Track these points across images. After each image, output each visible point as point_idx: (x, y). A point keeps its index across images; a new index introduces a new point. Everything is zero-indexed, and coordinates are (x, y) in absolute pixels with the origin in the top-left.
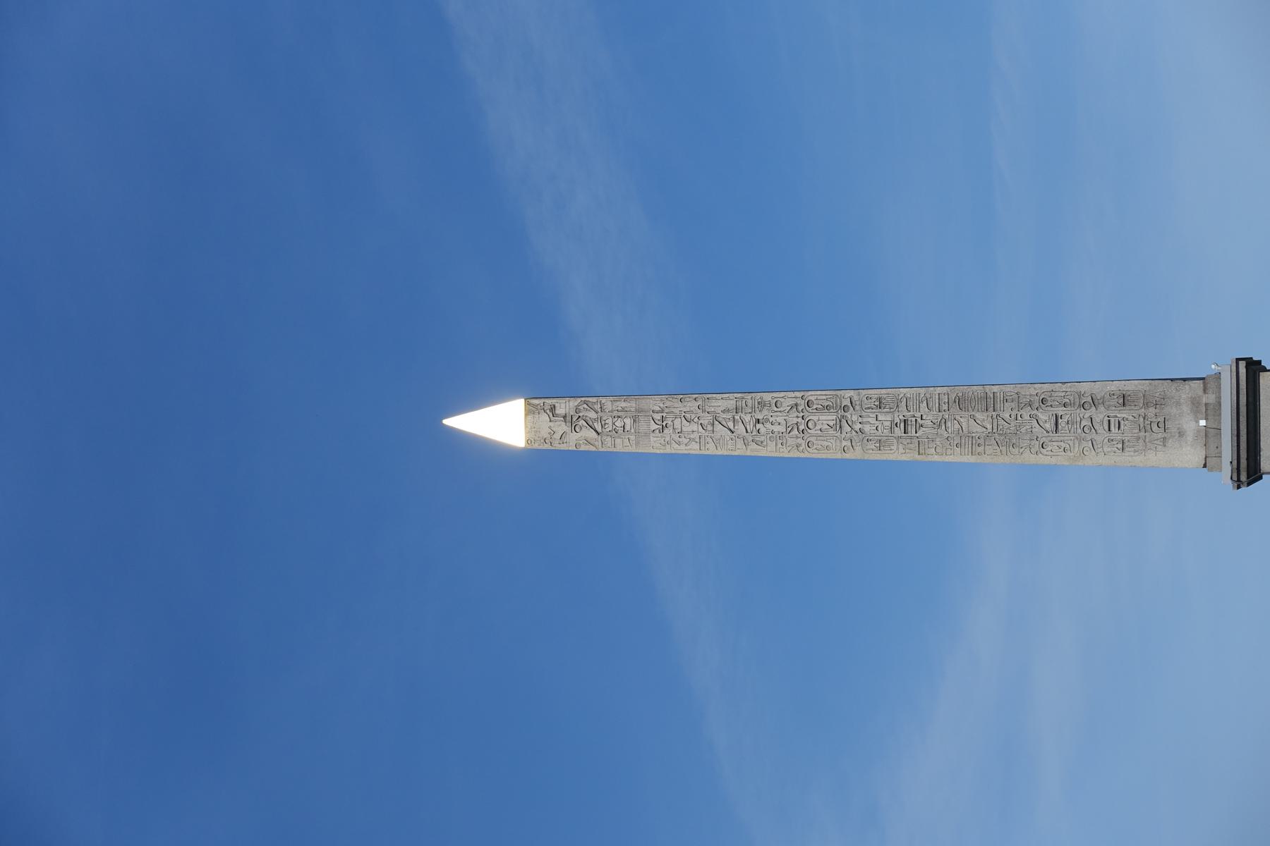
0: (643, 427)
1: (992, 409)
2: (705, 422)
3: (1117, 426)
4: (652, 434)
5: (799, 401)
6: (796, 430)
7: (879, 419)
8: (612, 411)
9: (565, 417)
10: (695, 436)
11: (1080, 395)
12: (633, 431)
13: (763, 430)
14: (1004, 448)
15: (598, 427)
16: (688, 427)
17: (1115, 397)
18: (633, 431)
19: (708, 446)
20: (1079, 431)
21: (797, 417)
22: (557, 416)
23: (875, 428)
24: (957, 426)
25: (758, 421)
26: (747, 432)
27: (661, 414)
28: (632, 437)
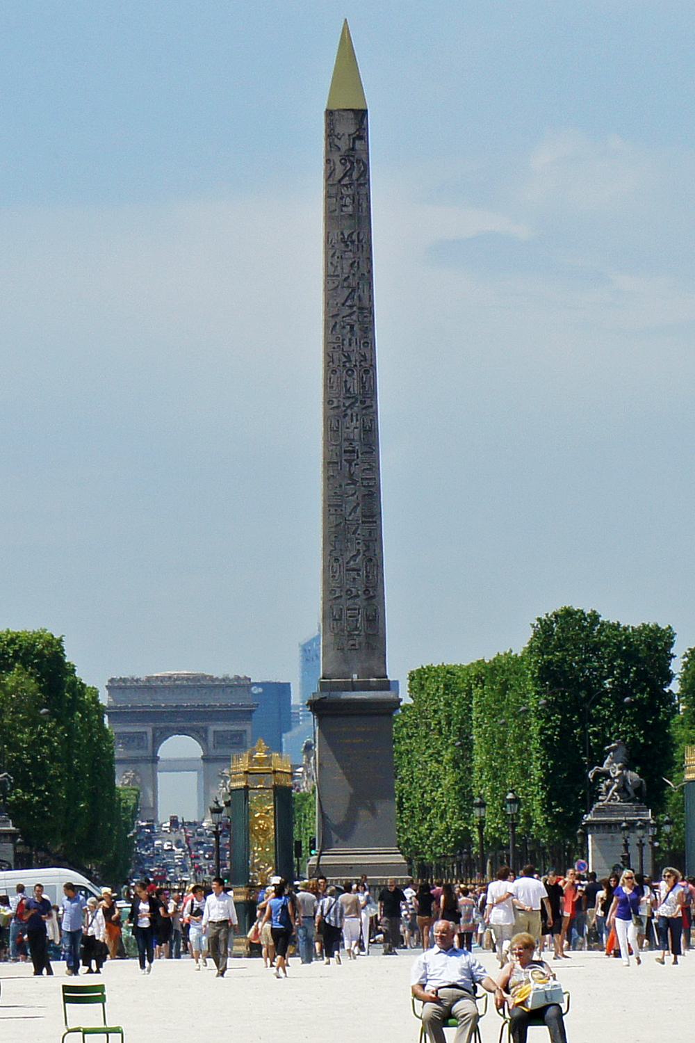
0: (346, 223)
1: (364, 519)
2: (350, 280)
3: (352, 615)
4: (339, 233)
5: (369, 362)
6: (345, 360)
7: (356, 430)
8: (358, 193)
9: (353, 149)
10: (339, 271)
11: (375, 587)
12: (343, 214)
13: (345, 331)
14: (333, 529)
15: (346, 181)
16: (346, 264)
17: (374, 613)
18: (343, 214)
19: (330, 282)
20: (348, 587)
21: (356, 361)
22: (354, 143)
23: (348, 425)
24: (350, 493)
25: (352, 327)
26: (343, 317)
27: (356, 240)
28: (336, 213)
